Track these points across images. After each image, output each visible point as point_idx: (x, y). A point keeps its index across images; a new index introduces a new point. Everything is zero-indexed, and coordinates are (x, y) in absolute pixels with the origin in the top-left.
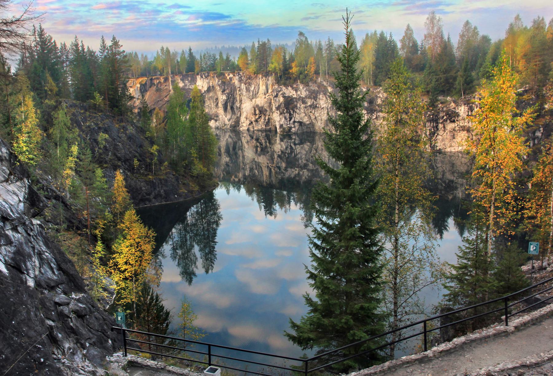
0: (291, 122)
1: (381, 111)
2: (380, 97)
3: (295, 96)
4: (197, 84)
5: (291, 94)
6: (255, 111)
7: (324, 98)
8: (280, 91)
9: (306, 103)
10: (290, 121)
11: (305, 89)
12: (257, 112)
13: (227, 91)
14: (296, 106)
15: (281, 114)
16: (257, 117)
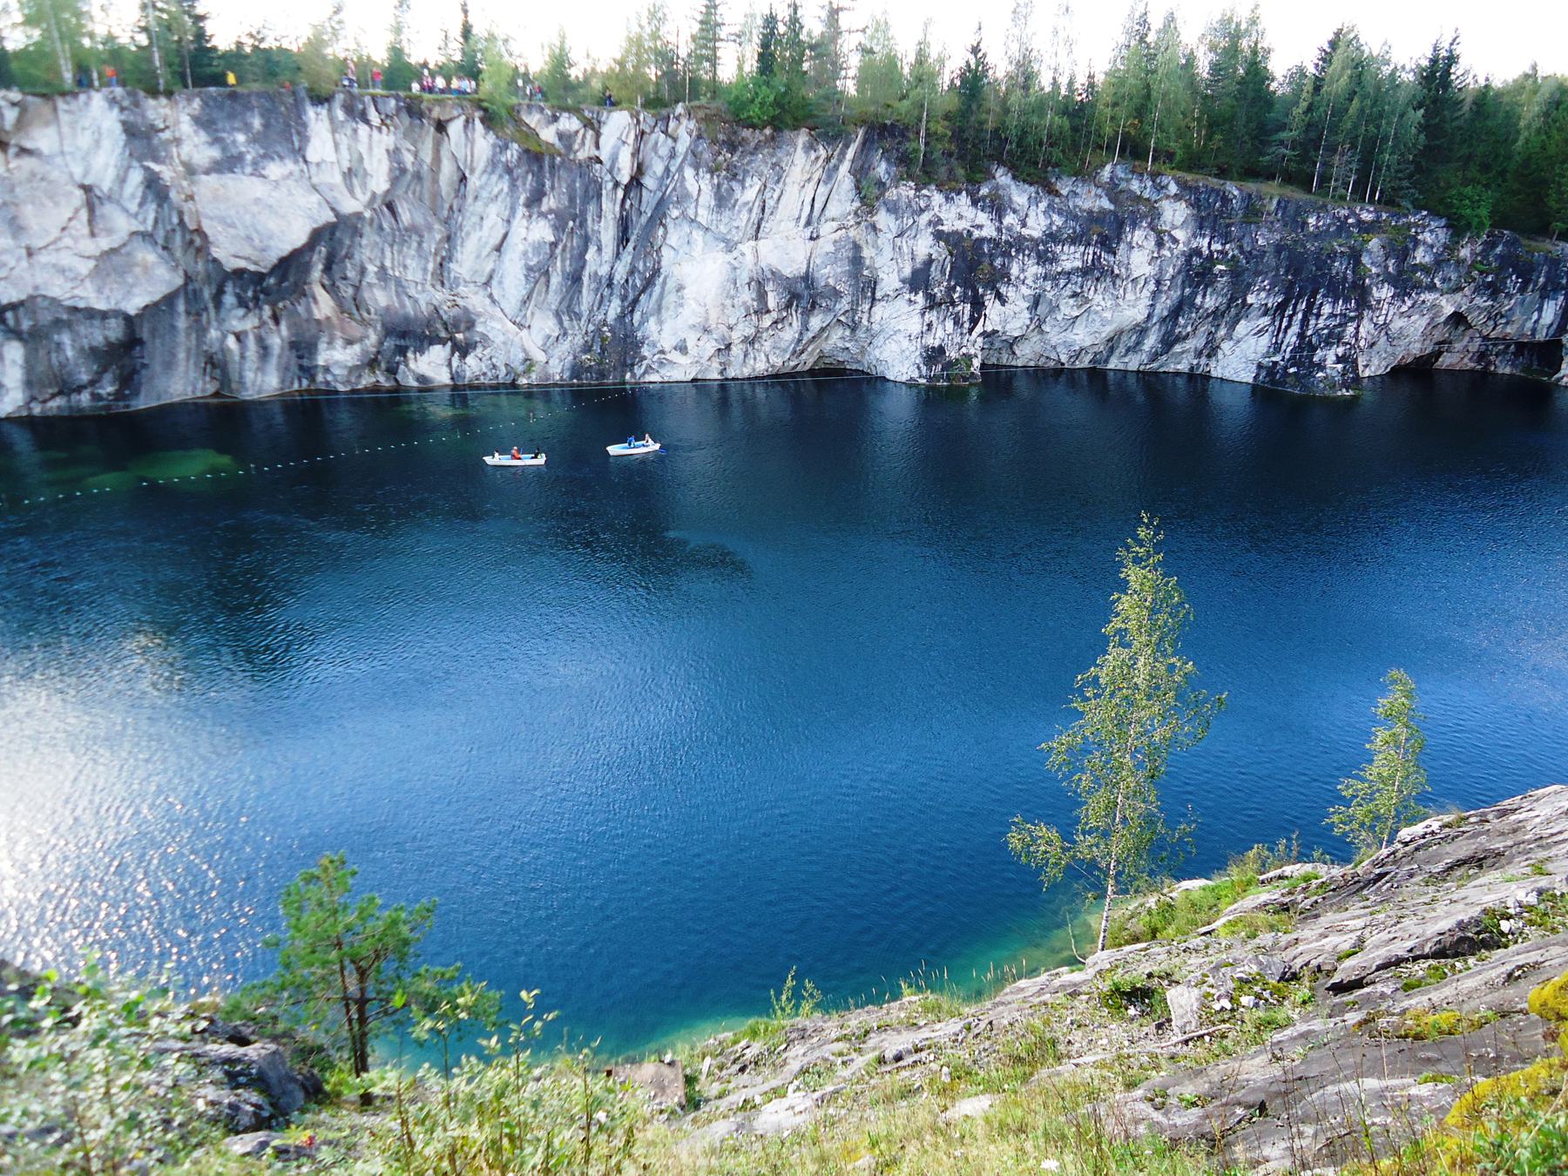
0: (974, 334)
1: (1432, 288)
2: (1425, 243)
3: (989, 231)
4: (312, 154)
5: (961, 226)
6: (762, 296)
7: (1151, 244)
8: (922, 211)
9: (1054, 260)
10: (971, 331)
11: (1043, 205)
12: (772, 301)
13: (549, 202)
14: (1005, 275)
15: (933, 304)
16: (767, 321)
